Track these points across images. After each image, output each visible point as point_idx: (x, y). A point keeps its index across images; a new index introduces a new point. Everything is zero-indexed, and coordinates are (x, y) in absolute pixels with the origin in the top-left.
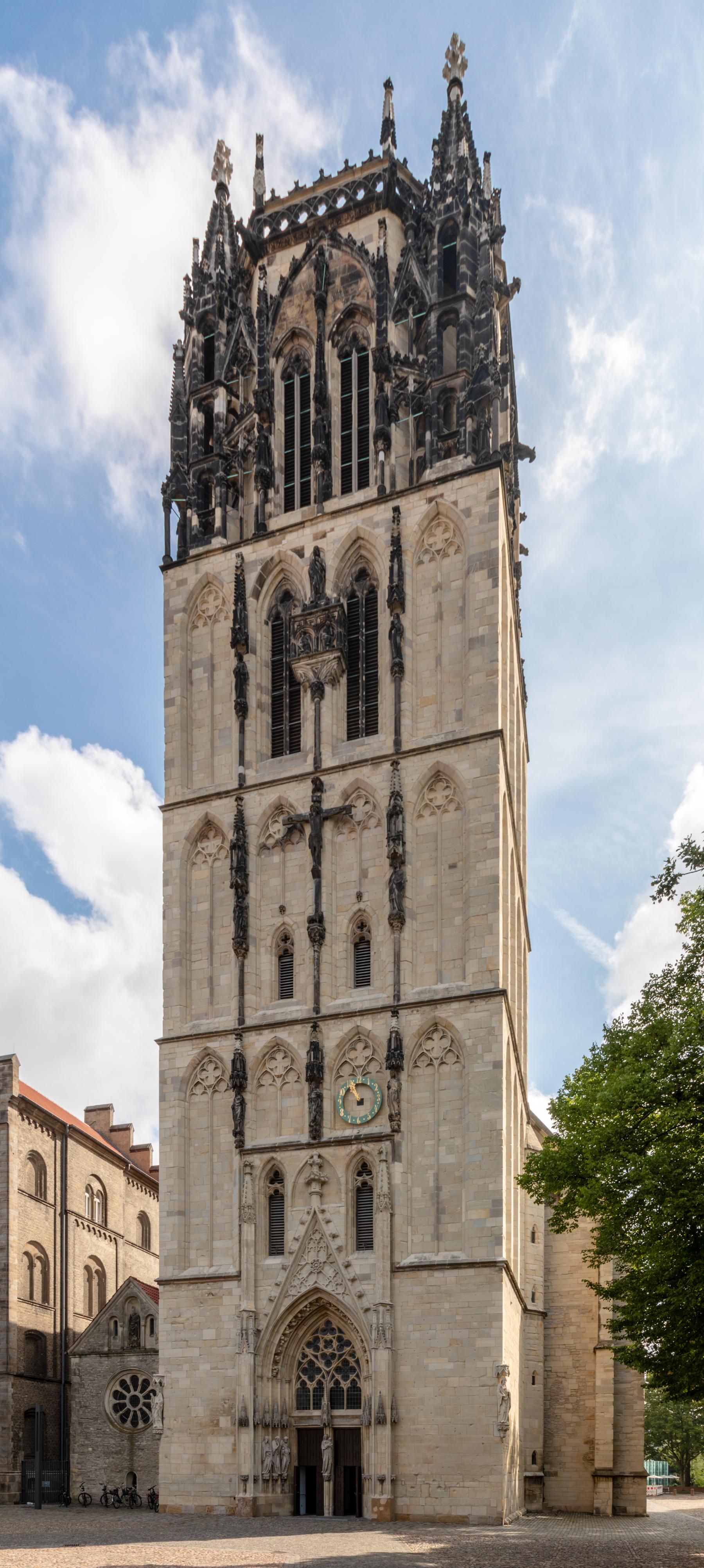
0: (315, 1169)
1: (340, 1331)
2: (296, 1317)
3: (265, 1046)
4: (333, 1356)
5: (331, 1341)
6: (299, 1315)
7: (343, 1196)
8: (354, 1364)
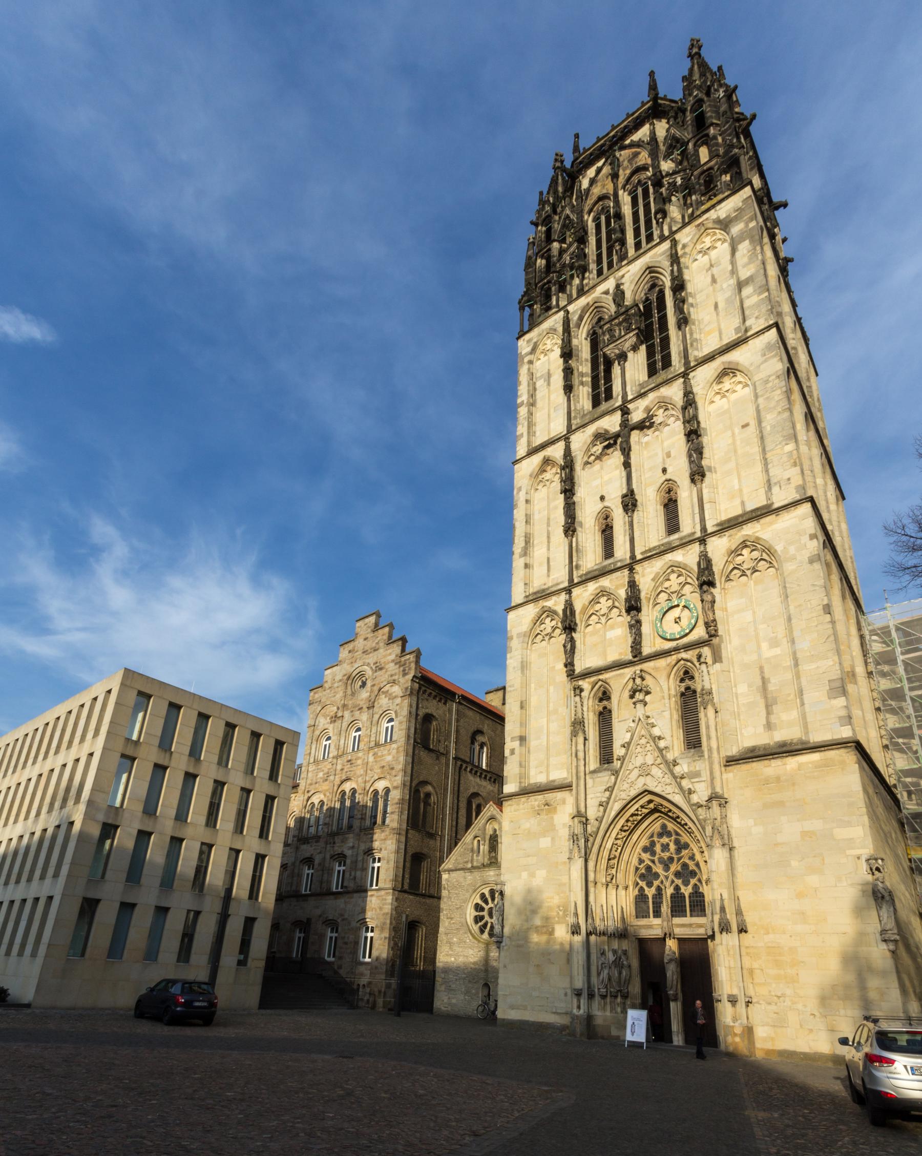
0: (638, 681)
1: (677, 834)
2: (627, 821)
3: (592, 594)
4: (671, 859)
5: (668, 845)
6: (631, 819)
7: (667, 701)
8: (695, 868)
